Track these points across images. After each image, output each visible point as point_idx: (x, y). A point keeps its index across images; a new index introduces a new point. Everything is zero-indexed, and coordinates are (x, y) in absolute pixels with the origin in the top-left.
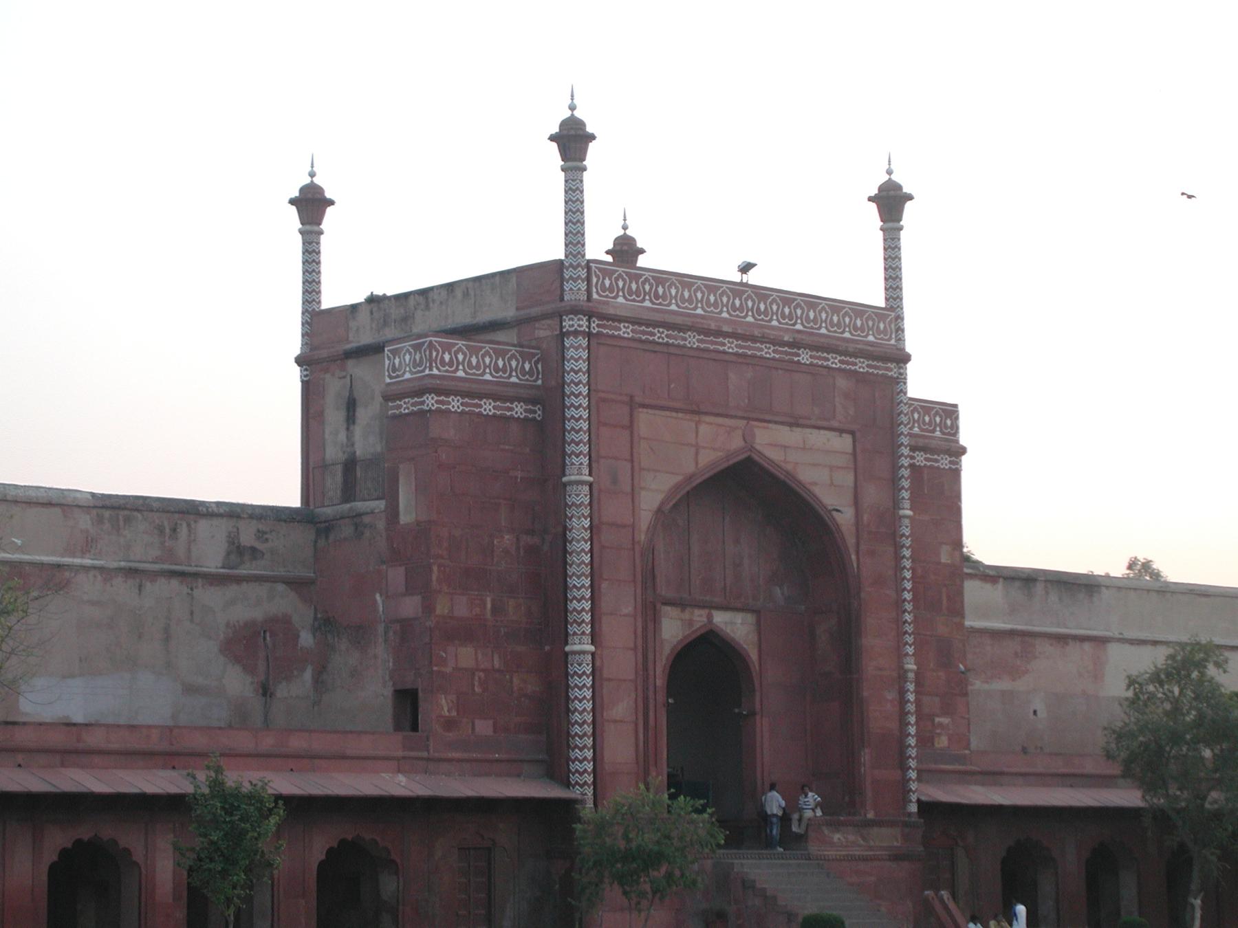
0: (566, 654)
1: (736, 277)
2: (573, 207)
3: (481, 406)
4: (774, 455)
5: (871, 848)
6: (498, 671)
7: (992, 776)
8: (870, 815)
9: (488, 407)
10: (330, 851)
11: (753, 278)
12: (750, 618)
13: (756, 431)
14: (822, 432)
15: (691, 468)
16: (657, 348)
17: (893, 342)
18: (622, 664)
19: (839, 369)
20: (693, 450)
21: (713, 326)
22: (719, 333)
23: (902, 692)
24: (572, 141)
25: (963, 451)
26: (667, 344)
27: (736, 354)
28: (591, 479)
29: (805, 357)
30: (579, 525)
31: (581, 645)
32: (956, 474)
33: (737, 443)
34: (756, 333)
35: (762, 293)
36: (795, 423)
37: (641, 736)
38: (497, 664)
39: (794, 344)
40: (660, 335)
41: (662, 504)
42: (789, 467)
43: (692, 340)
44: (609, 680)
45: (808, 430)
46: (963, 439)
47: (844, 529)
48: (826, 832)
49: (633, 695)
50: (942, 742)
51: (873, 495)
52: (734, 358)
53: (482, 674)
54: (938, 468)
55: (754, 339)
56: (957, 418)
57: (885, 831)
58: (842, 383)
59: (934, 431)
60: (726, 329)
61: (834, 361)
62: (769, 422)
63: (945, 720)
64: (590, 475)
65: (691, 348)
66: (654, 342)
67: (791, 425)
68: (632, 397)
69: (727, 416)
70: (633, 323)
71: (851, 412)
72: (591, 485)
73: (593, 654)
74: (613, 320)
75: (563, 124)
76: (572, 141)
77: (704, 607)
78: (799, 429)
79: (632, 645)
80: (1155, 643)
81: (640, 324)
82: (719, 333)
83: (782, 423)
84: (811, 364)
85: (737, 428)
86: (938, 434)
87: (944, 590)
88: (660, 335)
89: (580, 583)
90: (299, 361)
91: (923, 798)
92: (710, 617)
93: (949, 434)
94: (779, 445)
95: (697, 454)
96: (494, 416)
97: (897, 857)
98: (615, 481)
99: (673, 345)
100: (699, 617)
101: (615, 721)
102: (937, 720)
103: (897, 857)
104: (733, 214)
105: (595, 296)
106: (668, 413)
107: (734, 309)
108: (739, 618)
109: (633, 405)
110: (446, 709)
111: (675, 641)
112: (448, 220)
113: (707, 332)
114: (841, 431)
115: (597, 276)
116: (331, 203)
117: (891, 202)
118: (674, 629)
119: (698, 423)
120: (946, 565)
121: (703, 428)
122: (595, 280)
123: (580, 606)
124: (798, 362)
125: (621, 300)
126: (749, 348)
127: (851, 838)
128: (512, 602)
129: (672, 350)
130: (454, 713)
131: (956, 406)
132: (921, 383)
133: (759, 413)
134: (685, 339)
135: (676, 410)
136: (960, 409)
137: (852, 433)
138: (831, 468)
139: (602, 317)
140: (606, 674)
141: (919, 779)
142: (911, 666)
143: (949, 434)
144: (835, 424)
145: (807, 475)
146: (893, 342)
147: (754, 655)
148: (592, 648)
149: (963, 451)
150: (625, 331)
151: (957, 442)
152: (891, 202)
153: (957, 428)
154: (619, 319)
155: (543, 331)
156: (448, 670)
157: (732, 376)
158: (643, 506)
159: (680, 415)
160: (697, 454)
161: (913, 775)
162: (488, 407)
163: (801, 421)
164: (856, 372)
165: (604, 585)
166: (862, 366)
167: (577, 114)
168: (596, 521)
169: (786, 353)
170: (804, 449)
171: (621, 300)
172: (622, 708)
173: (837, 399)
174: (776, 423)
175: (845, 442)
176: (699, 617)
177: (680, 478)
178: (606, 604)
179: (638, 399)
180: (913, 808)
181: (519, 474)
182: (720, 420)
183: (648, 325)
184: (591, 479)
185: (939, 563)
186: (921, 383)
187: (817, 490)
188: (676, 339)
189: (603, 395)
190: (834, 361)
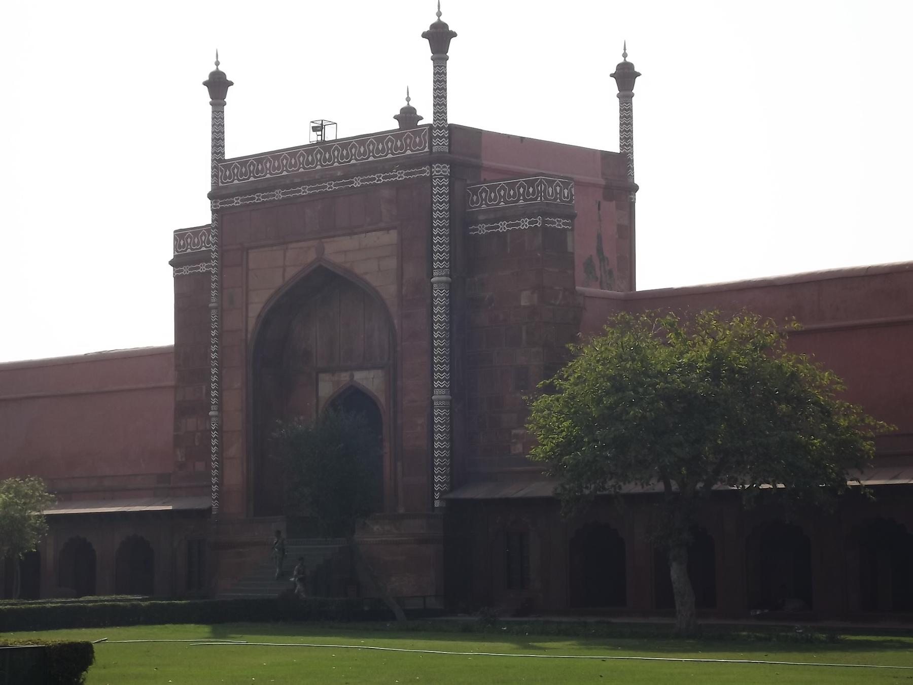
1: (314, 137)
3: (198, 268)
8: (401, 511)
11: (330, 135)
12: (380, 373)
14: (374, 233)
21: (288, 182)
23: (432, 416)
24: (218, 85)
27: (309, 195)
29: (357, 183)
33: (312, 256)
35: (345, 144)
36: (351, 232)
39: (345, 177)
40: (259, 198)
43: (279, 195)
60: (297, 180)
61: (379, 179)
62: (334, 236)
69: (305, 240)
76: (218, 85)
78: (356, 236)
83: (344, 235)
88: (259, 198)
90: (636, 188)
92: (352, 376)
93: (531, 200)
94: (342, 251)
95: (284, 271)
100: (344, 377)
102: (514, 432)
105: (220, 184)
107: (308, 163)
108: (372, 374)
114: (388, 229)
115: (222, 171)
116: (639, 75)
117: (439, 38)
125: (236, 182)
130: (184, 459)
134: (274, 195)
137: (394, 228)
143: (531, 200)
146: (427, 149)
152: (439, 38)
159: (274, 248)
166: (401, 176)
167: (442, 19)
172: (235, 449)
174: (339, 236)
176: (344, 377)
187: (367, 278)
190: (379, 179)
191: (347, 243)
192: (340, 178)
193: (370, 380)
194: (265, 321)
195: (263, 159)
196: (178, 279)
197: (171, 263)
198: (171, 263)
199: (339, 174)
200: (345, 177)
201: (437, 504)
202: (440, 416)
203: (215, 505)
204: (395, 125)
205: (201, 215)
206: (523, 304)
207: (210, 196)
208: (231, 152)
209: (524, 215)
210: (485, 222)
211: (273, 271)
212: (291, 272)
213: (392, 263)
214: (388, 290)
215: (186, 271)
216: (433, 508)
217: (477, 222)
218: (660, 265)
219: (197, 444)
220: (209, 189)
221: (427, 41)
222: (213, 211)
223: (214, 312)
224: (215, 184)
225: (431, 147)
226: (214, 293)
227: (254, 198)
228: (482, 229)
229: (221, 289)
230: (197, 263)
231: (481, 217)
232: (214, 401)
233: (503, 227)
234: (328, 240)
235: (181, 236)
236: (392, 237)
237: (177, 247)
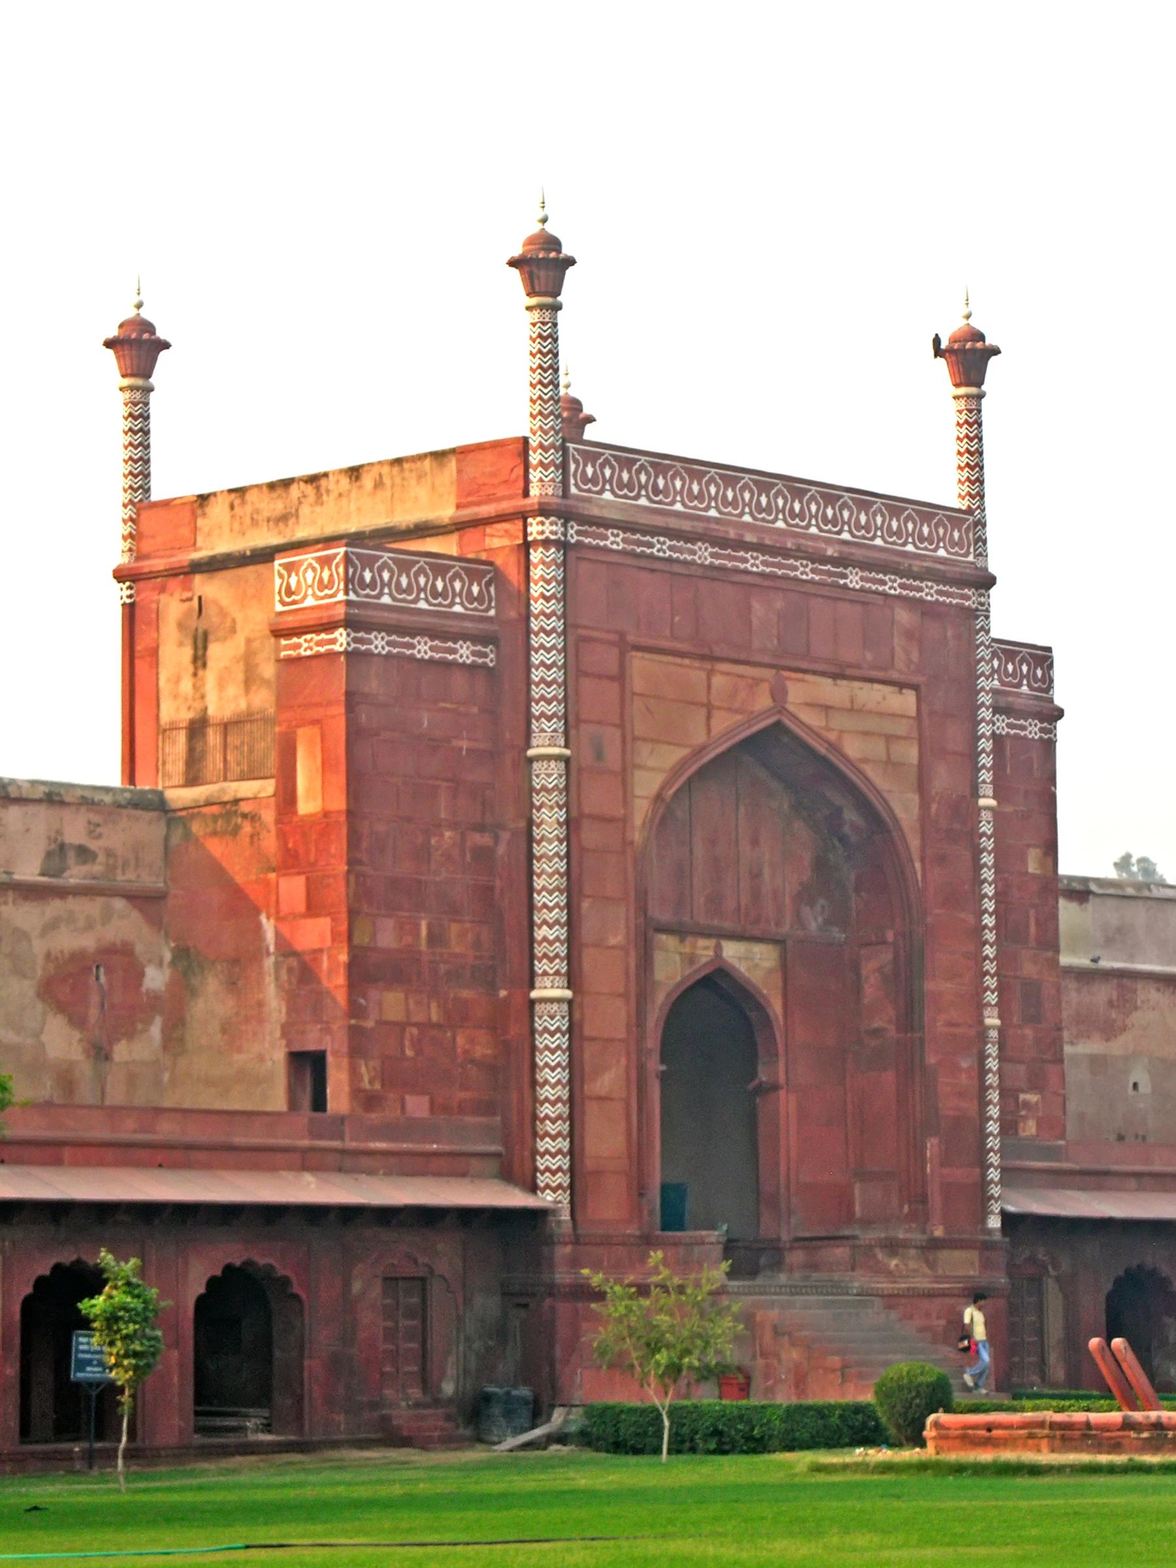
0: (532, 1003)
3: (413, 646)
4: (813, 719)
5: (938, 1279)
6: (439, 1026)
7: (1096, 1179)
9: (423, 649)
10: (212, 1283)
13: (789, 684)
14: (876, 686)
15: (700, 738)
16: (657, 565)
17: (971, 558)
18: (611, 1017)
19: (899, 597)
20: (704, 711)
21: (732, 534)
23: (982, 1057)
25: (1060, 713)
26: (670, 560)
27: (762, 575)
28: (567, 752)
29: (854, 579)
30: (549, 820)
31: (550, 989)
32: (1048, 747)
34: (789, 545)
37: (634, 1119)
38: (435, 1015)
39: (842, 561)
40: (661, 547)
41: (663, 788)
43: (704, 554)
44: (593, 1039)
45: (857, 684)
46: (1059, 698)
48: (880, 1256)
49: (623, 1061)
50: (1029, 1128)
52: (759, 581)
53: (415, 1031)
54: (1025, 737)
55: (785, 553)
56: (1051, 666)
57: (958, 1255)
58: (903, 616)
59: (1019, 685)
60: (749, 538)
61: (892, 586)
62: (805, 671)
63: (1033, 1098)
64: (566, 746)
65: (702, 565)
66: (652, 557)
68: (622, 635)
70: (625, 530)
72: (567, 761)
73: (570, 1002)
74: (599, 525)
75: (530, 241)
76: (543, 267)
77: (709, 936)
78: (844, 683)
79: (622, 990)
81: (634, 531)
82: (740, 545)
83: (823, 674)
84: (862, 590)
85: (762, 680)
86: (1025, 689)
87: (1032, 912)
88: (661, 547)
89: (549, 899)
91: (1011, 1209)
92: (718, 949)
95: (709, 717)
96: (431, 661)
98: (599, 755)
99: (677, 561)
100: (704, 949)
101: (600, 1099)
102: (1022, 1097)
104: (754, 373)
105: (573, 490)
106: (670, 659)
109: (624, 647)
110: (366, 1079)
111: (671, 984)
112: (358, 376)
114: (901, 686)
115: (576, 462)
118: (672, 965)
119: (710, 673)
120: (1034, 876)
122: (573, 467)
123: (549, 933)
124: (845, 586)
125: (607, 496)
126: (780, 566)
128: (455, 928)
129: (676, 568)
130: (378, 1086)
131: (1049, 649)
132: (1010, 617)
133: (791, 662)
134: (694, 553)
135: (682, 655)
136: (1055, 653)
137: (915, 687)
138: (889, 738)
139: (584, 520)
140: (587, 1031)
141: (1001, 1182)
142: (992, 1020)
144: (895, 675)
146: (971, 558)
147: (776, 1007)
148: (568, 994)
149: (1060, 713)
150: (615, 541)
151: (1051, 701)
152: (969, 358)
153: (1051, 681)
155: (498, 541)
156: (370, 1024)
157: (756, 605)
158: (638, 791)
159: (686, 661)
160: (709, 717)
161: (994, 1174)
162: (423, 649)
163: (849, 672)
164: (921, 601)
165: (585, 905)
166: (929, 592)
168: (574, 814)
169: (830, 574)
170: (851, 710)
171: (607, 496)
173: (896, 640)
174: (815, 673)
175: (907, 701)
178: (588, 930)
179: (631, 638)
180: (994, 1222)
181: (465, 744)
183: (644, 533)
184: (567, 752)
185: (1027, 873)
186: (1010, 617)
189: (582, 632)
190: (892, 586)
193: (751, 961)
195: (671, 467)
219: (409, 1053)
223: (986, 816)
227: (651, 546)
234: (793, 675)
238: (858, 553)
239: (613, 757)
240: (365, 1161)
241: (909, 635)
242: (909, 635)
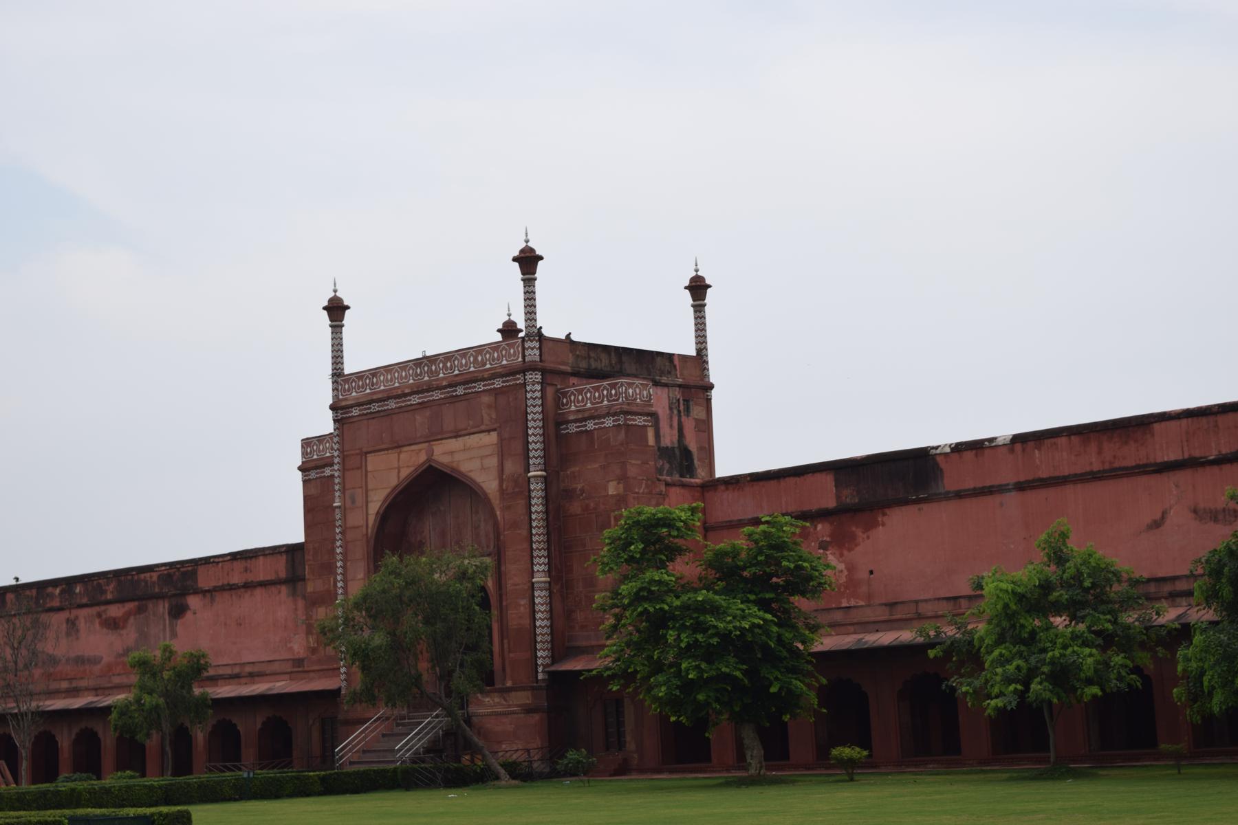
2: (530, 303)
4: (445, 460)
5: (509, 706)
8: (509, 684)
10: (263, 723)
15: (394, 482)
22: (405, 395)
24: (336, 309)
29: (460, 391)
33: (423, 458)
36: (457, 435)
39: (450, 386)
40: (375, 407)
42: (455, 465)
43: (392, 404)
47: (491, 496)
51: (511, 467)
55: (428, 391)
57: (519, 693)
58: (486, 399)
60: (407, 391)
61: (480, 387)
67: (456, 437)
71: (494, 416)
75: (331, 300)
76: (336, 309)
80: (959, 495)
82: (405, 395)
86: (605, 402)
88: (375, 407)
94: (447, 453)
97: (528, 710)
98: (353, 502)
103: (528, 710)
107: (417, 375)
113: (398, 397)
114: (489, 431)
117: (528, 261)
119: (399, 454)
121: (402, 456)
127: (497, 700)
135: (387, 449)
137: (494, 430)
138: (482, 458)
144: (483, 427)
145: (464, 468)
152: (528, 261)
154: (352, 406)
157: (418, 417)
166: (498, 383)
175: (493, 437)
177: (389, 490)
182: (413, 447)
187: (472, 475)
188: (425, 397)
191: (453, 444)
192: (445, 387)
194: (385, 517)
196: (305, 482)
197: (300, 469)
198: (300, 469)
199: (444, 383)
200: (450, 386)
201: (540, 677)
202: (540, 597)
203: (344, 684)
204: (498, 337)
205: (324, 424)
206: (611, 492)
207: (332, 408)
208: (349, 368)
209: (608, 414)
210: (576, 421)
211: (387, 473)
212: (405, 473)
213: (493, 462)
214: (489, 484)
215: (313, 475)
216: (537, 681)
217: (568, 422)
218: (734, 455)
220: (330, 401)
221: (517, 264)
222: (335, 421)
223: (337, 511)
224: (335, 397)
225: (524, 356)
226: (337, 494)
228: (573, 428)
229: (343, 490)
230: (320, 469)
231: (572, 417)
232: (340, 591)
233: (590, 425)
235: (307, 443)
236: (493, 437)
237: (304, 454)
238: (375, 397)
239: (360, 500)
240: (312, 674)
241: (489, 406)
242: (489, 406)
